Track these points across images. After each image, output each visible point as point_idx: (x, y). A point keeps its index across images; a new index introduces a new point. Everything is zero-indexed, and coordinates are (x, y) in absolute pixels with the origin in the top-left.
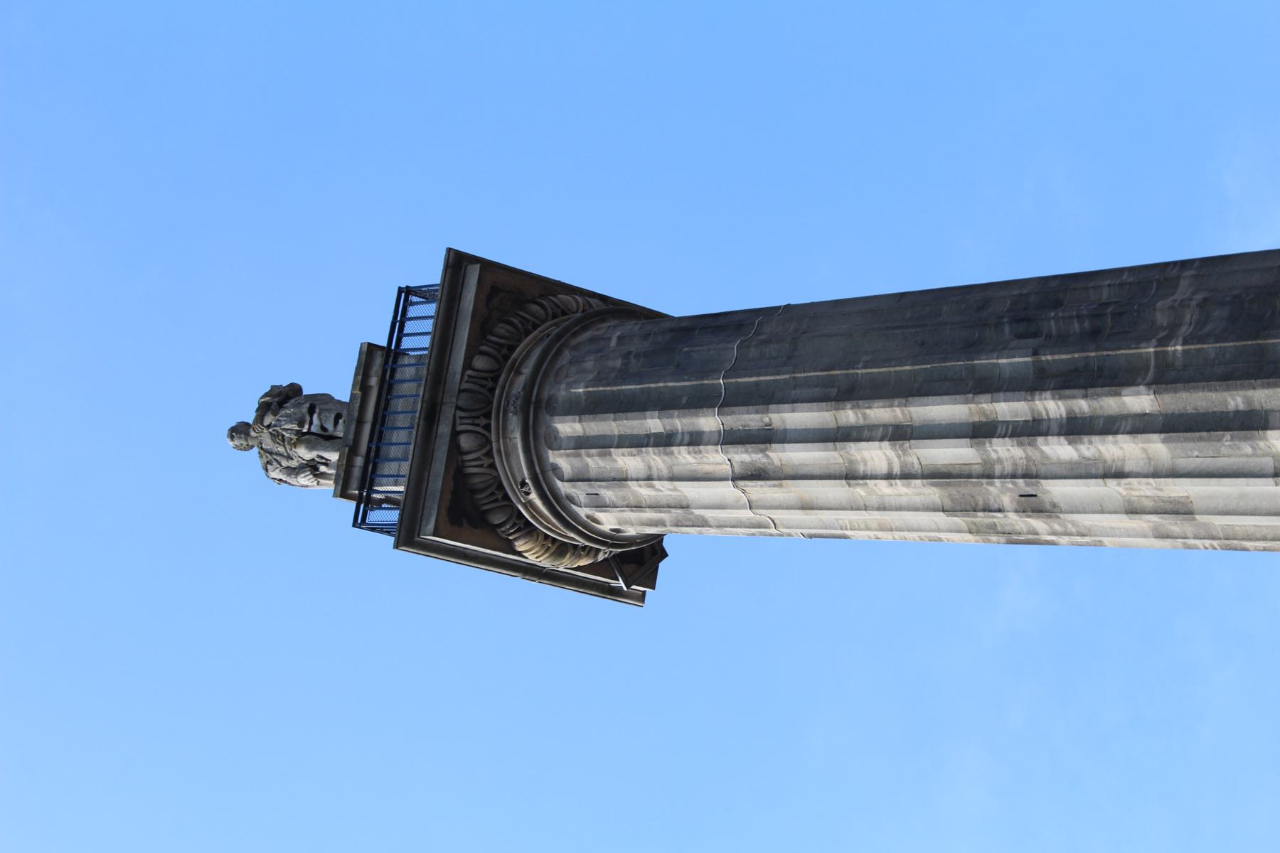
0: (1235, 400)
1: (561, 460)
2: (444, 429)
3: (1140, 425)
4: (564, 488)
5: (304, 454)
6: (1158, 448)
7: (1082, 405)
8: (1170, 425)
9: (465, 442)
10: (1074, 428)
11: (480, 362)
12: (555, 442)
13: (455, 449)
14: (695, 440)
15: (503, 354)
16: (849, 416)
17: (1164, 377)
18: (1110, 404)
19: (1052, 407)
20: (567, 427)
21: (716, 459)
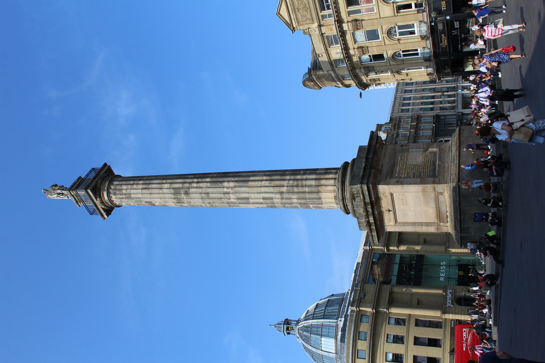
0: (221, 180)
1: (112, 187)
2: (96, 180)
4: (111, 191)
5: (59, 191)
6: (209, 185)
7: (200, 180)
10: (197, 182)
12: (113, 184)
13: (97, 182)
14: (138, 184)
18: (204, 180)
19: (196, 180)
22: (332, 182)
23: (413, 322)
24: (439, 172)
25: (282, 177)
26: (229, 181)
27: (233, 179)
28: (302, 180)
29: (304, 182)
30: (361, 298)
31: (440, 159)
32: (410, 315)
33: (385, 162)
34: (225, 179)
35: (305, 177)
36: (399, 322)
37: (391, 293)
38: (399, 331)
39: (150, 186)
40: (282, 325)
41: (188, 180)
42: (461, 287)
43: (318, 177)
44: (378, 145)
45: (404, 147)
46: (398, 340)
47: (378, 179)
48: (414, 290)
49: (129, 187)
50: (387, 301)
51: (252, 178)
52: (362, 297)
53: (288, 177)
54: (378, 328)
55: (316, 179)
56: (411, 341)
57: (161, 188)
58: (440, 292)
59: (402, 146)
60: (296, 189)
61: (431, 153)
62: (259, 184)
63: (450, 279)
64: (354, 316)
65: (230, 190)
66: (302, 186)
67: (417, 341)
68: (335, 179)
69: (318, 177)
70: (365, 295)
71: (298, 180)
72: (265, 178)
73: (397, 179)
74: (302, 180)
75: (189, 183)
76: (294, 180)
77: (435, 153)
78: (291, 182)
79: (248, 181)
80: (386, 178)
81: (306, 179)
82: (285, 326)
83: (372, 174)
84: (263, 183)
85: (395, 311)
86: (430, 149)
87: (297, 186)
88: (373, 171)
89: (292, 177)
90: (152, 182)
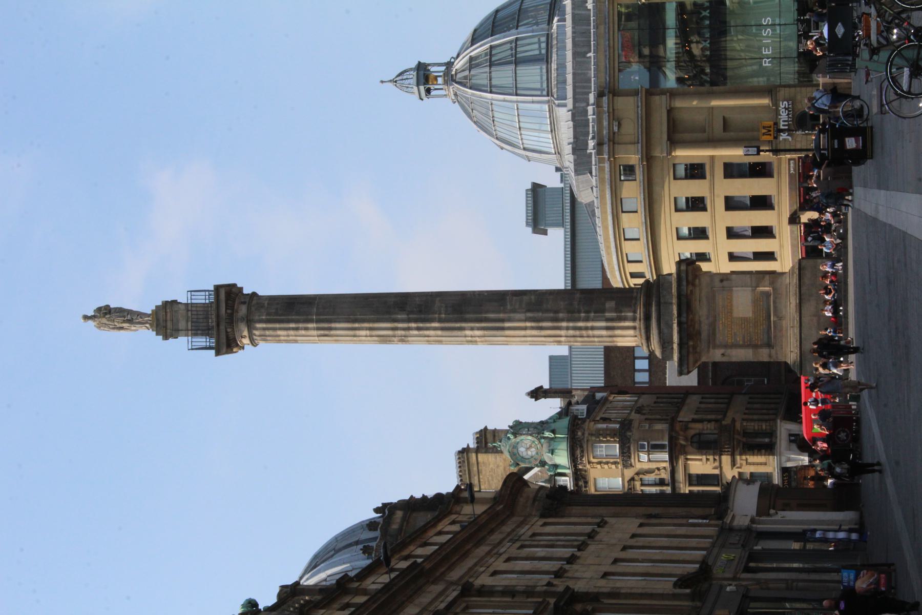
0: (458, 325)
2: (222, 327)
3: (435, 329)
7: (421, 325)
8: (442, 329)
9: (229, 330)
10: (418, 329)
11: (229, 311)
13: (227, 332)
15: (232, 308)
16: (357, 325)
17: (440, 321)
18: (428, 325)
19: (413, 325)
20: (259, 325)
21: (315, 333)
22: (631, 332)
23: (719, 171)
24: (775, 337)
25: (556, 324)
26: (472, 329)
27: (477, 325)
28: (586, 328)
29: (590, 332)
30: (614, 133)
31: (775, 315)
32: (712, 158)
33: (702, 312)
34: (464, 325)
35: (589, 324)
36: (695, 171)
37: (670, 111)
38: (695, 188)
39: (333, 332)
40: (416, 88)
41: (400, 325)
42: (803, 89)
43: (610, 324)
44: (690, 288)
45: (725, 283)
46: (696, 204)
47: (698, 349)
48: (715, 103)
49: (292, 332)
50: (665, 137)
51: (507, 325)
52: (616, 129)
53: (564, 324)
54: (656, 189)
55: (607, 328)
56: (720, 204)
57: (354, 336)
58: (766, 101)
59: (722, 281)
60: (579, 339)
61: (763, 293)
62: (522, 333)
63: (782, 61)
64: (607, 169)
65: (477, 339)
66: (588, 336)
67: (732, 204)
68: (634, 328)
69: (610, 324)
70: (619, 125)
71: (580, 328)
72: (528, 324)
73: (722, 351)
74: (586, 328)
75: (404, 329)
76: (575, 328)
77: (767, 294)
78: (571, 332)
79: (503, 329)
80: (709, 347)
81: (593, 328)
82: (422, 88)
83: (691, 349)
84: (529, 332)
85: (686, 154)
86: (761, 289)
87: (582, 336)
88: (691, 343)
89: (571, 324)
90: (333, 325)
